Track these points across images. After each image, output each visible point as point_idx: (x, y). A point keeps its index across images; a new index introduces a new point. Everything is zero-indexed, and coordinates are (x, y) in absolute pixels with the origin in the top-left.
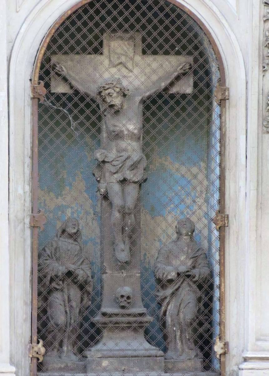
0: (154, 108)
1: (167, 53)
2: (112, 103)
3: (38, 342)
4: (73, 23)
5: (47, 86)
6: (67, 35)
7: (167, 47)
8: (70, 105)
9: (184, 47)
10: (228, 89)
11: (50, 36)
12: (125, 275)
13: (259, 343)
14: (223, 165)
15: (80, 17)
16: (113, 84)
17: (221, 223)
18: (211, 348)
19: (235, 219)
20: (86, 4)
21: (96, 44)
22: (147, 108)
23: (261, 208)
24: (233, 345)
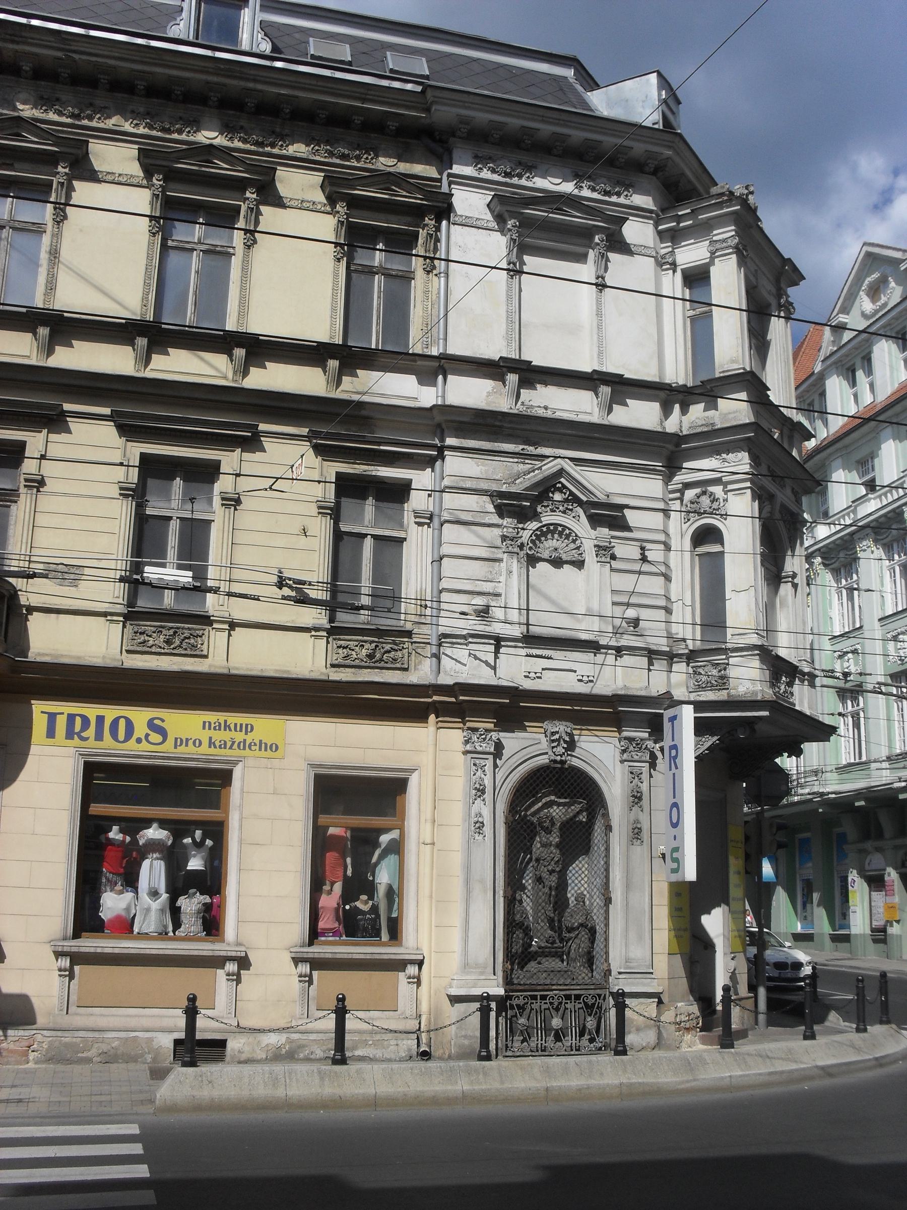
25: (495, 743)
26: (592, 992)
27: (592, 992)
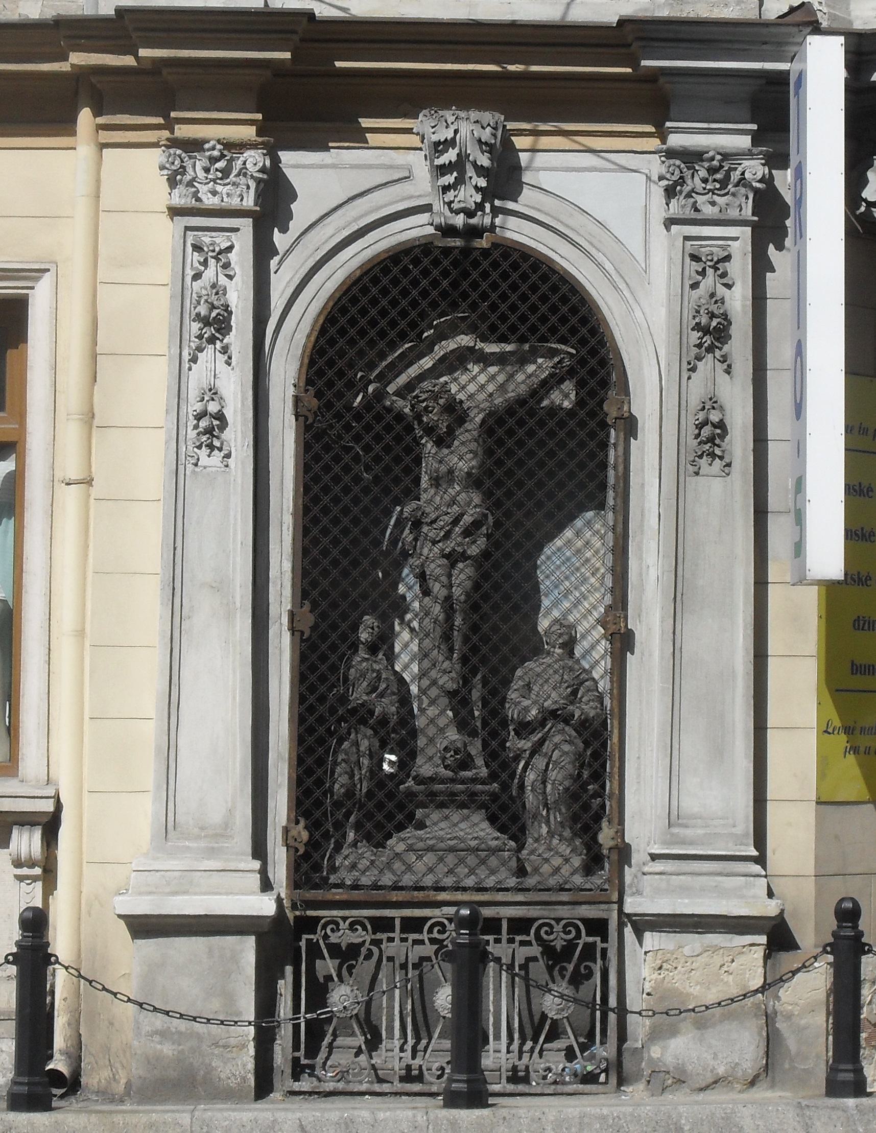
0: (500, 432)
3: (297, 822)
5: (319, 395)
6: (354, 310)
11: (326, 313)
13: (675, 830)
19: (640, 621)
20: (385, 259)
21: (403, 324)
25: (756, 191)
26: (563, 912)
27: (563, 912)
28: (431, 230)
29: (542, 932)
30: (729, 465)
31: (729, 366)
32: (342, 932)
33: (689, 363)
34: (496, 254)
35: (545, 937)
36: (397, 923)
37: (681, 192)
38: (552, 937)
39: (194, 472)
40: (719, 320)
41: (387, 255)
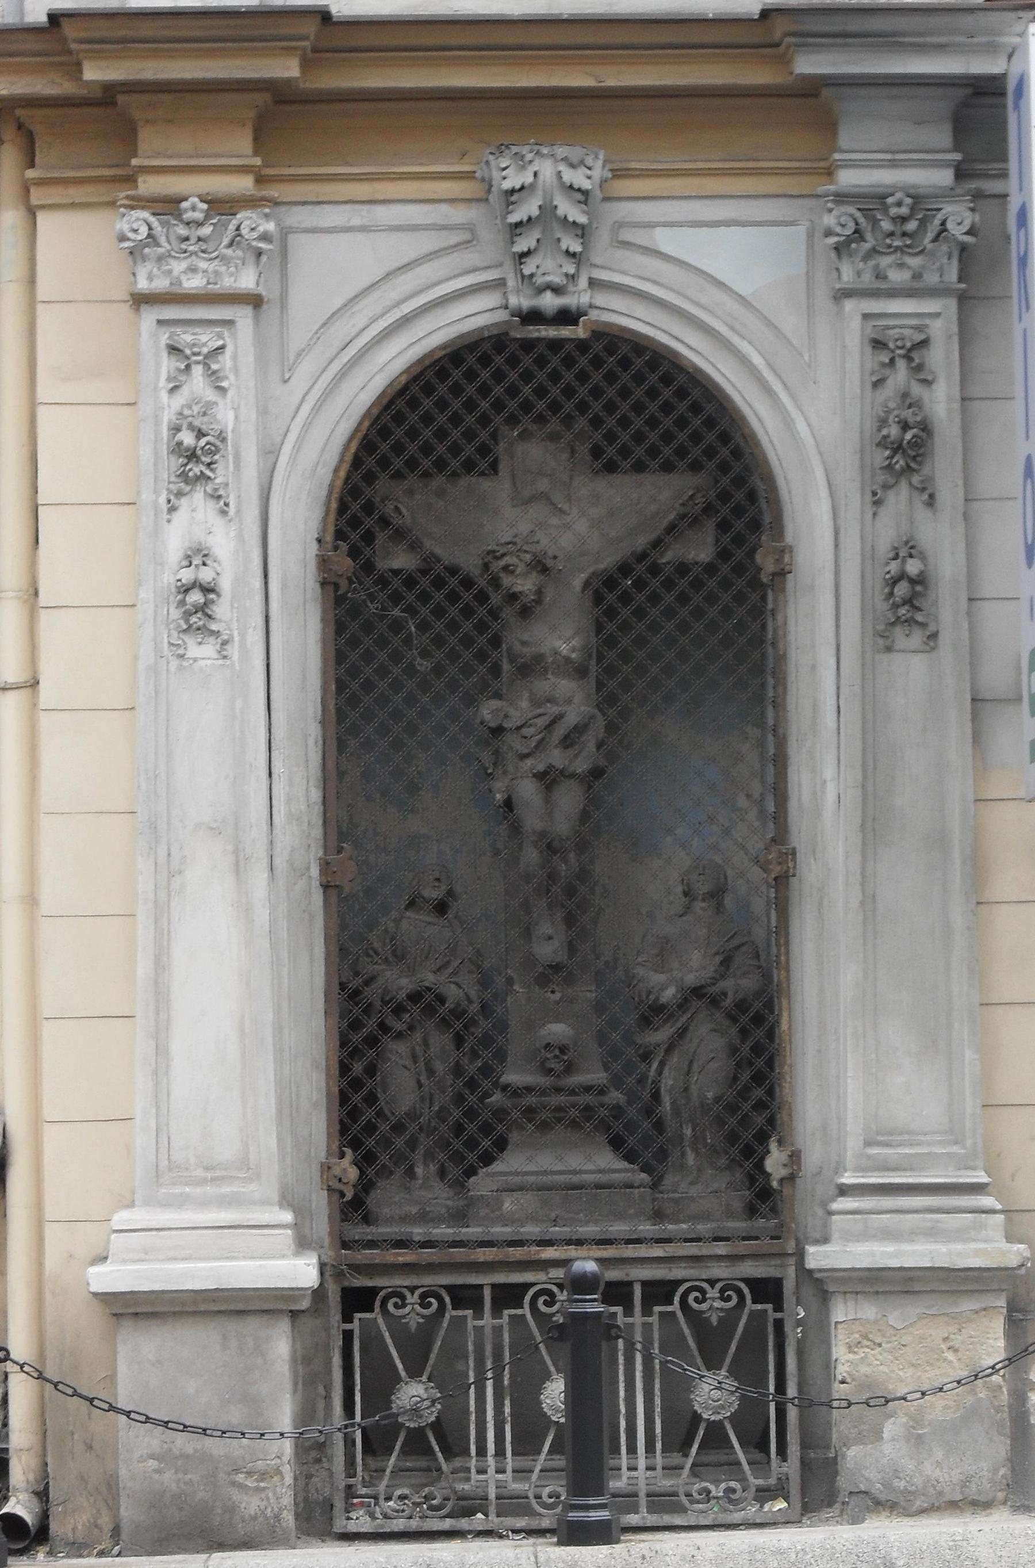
1: (639, 467)
2: (517, 589)
3: (342, 1156)
4: (413, 404)
5: (354, 553)
6: (399, 432)
7: (639, 451)
8: (410, 597)
9: (681, 452)
10: (791, 549)
11: (360, 436)
12: (557, 996)
14: (781, 731)
15: (428, 390)
16: (515, 544)
17: (779, 868)
18: (760, 1166)
19: (815, 859)
20: (441, 358)
21: (469, 450)
22: (598, 599)
23: (874, 830)
24: (813, 1158)
26: (719, 1271)
28: (502, 316)
29: (691, 1299)
30: (934, 636)
31: (932, 496)
32: (408, 1308)
33: (874, 494)
34: (598, 347)
35: (695, 1306)
36: (487, 1293)
37: (857, 250)
38: (704, 1306)
39: (181, 668)
40: (915, 431)
41: (444, 352)
